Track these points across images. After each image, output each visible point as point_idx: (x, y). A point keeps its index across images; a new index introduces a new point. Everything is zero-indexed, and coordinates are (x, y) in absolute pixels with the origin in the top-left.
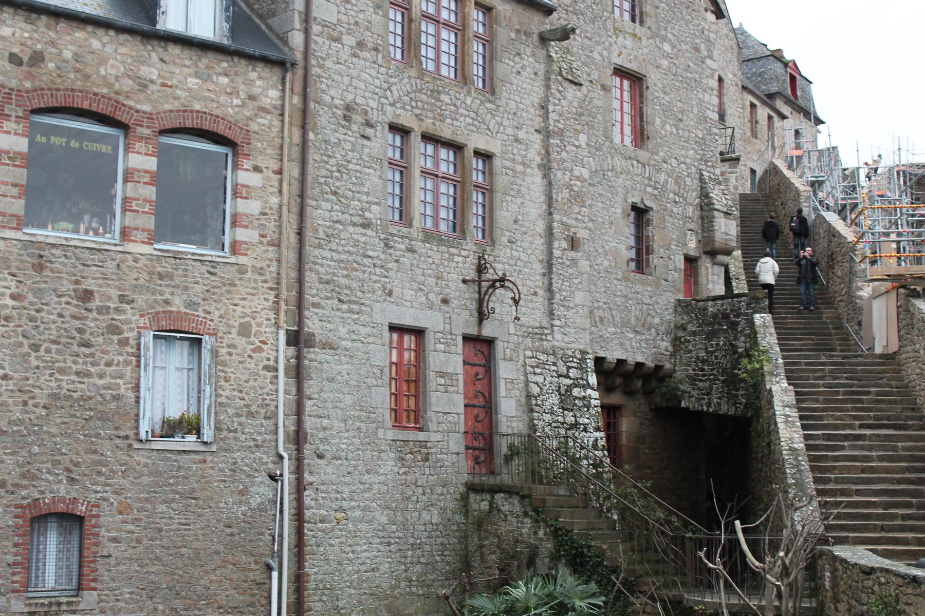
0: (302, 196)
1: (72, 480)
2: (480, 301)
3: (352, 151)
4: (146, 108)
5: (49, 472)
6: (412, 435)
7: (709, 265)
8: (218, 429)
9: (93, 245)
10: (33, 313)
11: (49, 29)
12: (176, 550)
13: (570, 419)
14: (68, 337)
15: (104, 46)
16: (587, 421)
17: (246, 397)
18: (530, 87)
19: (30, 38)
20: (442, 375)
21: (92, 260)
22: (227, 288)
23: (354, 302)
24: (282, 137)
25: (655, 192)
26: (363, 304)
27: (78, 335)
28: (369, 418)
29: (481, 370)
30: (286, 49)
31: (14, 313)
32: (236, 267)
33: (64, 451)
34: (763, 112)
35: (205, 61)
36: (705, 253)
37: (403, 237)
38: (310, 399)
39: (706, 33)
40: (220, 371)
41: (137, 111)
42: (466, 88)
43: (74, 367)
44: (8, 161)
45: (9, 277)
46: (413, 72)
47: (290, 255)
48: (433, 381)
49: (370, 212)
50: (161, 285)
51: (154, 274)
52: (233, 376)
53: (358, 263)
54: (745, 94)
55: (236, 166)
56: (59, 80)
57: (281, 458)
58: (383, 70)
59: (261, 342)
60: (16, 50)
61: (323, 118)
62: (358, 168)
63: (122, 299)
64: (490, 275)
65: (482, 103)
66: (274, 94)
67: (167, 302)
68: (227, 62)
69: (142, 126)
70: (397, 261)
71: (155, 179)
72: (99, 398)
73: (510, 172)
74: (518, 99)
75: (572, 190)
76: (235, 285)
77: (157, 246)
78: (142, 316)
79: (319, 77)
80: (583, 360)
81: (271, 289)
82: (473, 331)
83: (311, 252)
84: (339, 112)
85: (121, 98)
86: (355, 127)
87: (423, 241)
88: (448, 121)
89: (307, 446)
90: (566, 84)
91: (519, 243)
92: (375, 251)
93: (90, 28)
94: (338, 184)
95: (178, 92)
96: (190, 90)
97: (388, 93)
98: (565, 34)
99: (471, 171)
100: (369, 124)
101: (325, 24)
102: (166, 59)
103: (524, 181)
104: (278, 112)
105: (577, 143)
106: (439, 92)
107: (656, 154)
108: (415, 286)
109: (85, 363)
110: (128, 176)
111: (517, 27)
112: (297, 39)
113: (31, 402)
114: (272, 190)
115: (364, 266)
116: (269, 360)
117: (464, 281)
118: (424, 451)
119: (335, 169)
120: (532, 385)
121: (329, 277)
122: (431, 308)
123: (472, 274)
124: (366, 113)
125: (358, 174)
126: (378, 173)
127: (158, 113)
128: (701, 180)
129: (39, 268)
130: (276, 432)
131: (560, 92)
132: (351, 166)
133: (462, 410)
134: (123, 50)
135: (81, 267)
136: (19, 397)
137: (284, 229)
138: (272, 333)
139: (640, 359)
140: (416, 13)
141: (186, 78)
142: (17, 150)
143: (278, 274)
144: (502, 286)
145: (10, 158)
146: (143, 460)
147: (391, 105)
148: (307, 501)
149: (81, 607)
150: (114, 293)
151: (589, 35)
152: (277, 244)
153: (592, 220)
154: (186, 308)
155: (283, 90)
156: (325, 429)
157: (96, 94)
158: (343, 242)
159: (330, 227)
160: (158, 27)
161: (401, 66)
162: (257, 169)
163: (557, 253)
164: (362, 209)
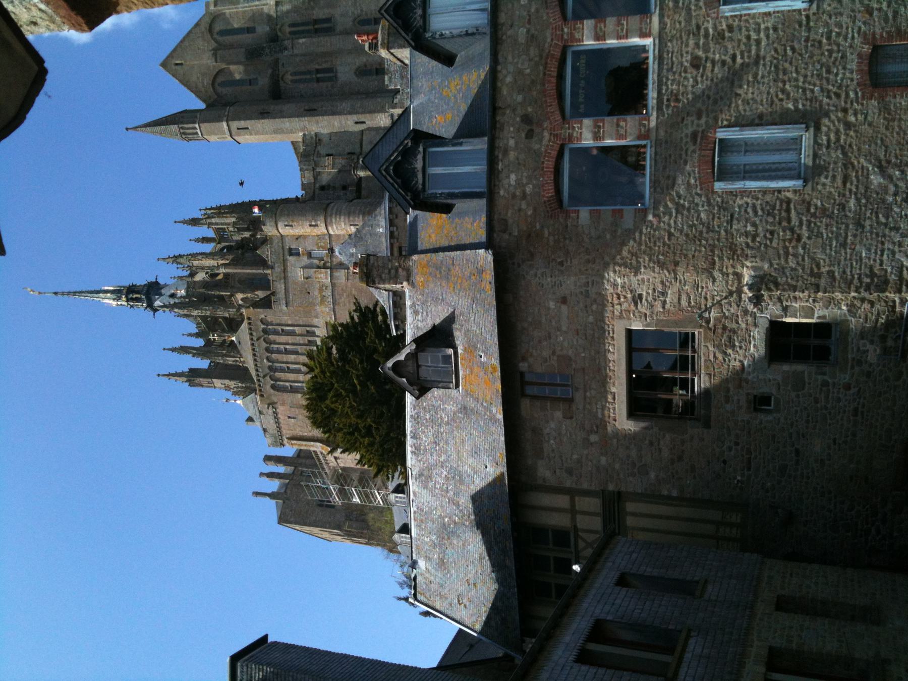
10: (711, 101)
19: (513, 126)
41: (552, 40)
60: (523, 135)
69: (562, 35)
77: (653, 6)
93: (499, 84)
95: (533, 10)
134: (510, 58)
141: (522, 5)
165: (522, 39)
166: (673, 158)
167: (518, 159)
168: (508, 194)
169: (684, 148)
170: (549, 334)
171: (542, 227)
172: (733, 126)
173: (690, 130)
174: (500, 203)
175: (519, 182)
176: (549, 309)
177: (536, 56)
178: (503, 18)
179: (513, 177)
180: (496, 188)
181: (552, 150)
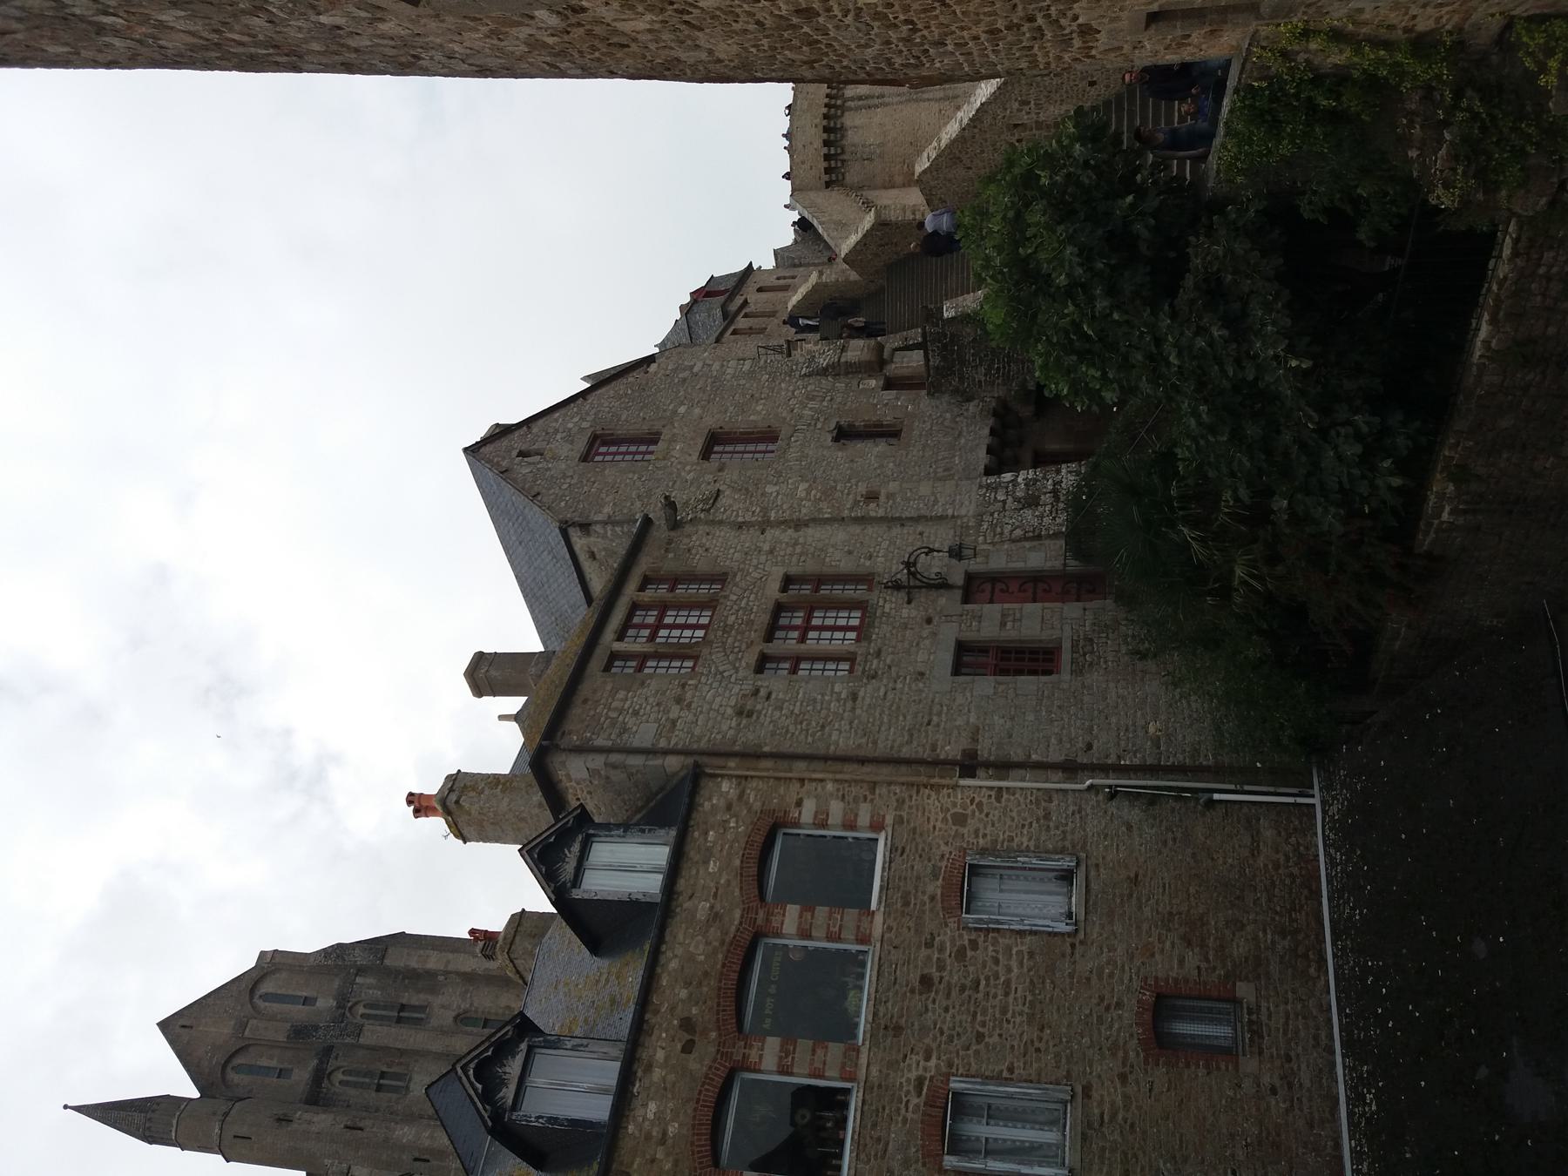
0: (826, 759)
1: (1119, 1005)
2: (930, 587)
3: (782, 709)
4: (737, 914)
5: (1111, 1027)
6: (1066, 656)
7: (893, 366)
8: (1062, 851)
9: (875, 973)
12: (1192, 899)
13: (1047, 498)
14: (969, 1002)
15: (676, 956)
16: (1050, 482)
17: (1029, 821)
18: (720, 539)
19: (666, 1032)
20: (1003, 624)
21: (890, 974)
22: (917, 836)
23: (931, 708)
24: (768, 777)
25: (822, 420)
26: (933, 701)
27: (967, 993)
28: (1049, 697)
29: (999, 586)
30: (682, 774)
31: (944, 1058)
32: (896, 826)
33: (1087, 1012)
34: (741, 323)
35: (692, 854)
36: (881, 370)
37: (866, 662)
38: (1030, 756)
39: (668, 372)
40: (1002, 846)
41: (741, 923)
42: (721, 600)
43: (1000, 997)
44: (790, 1059)
45: (908, 1061)
46: (705, 651)
47: (885, 772)
48: (1011, 633)
49: (841, 693)
50: (915, 904)
51: (903, 912)
52: (1007, 833)
53: (892, 705)
54: (723, 340)
55: (797, 825)
56: (709, 1003)
57: (1091, 787)
58: (703, 679)
59: (972, 804)
60: (679, 1047)
61: (750, 737)
62: (798, 704)
63: (929, 945)
64: (903, 576)
65: (736, 585)
66: (725, 786)
67: (933, 898)
68: (694, 831)
70: (890, 667)
71: (808, 908)
72: (1032, 973)
73: (803, 559)
74: (732, 551)
75: (820, 499)
76: (915, 829)
78: (946, 925)
79: (709, 741)
80: (988, 486)
81: (918, 792)
82: (958, 594)
83: (882, 749)
84: (744, 722)
85: (728, 940)
86: (759, 707)
87: (870, 643)
88: (752, 617)
89: (1079, 760)
90: (718, 505)
91: (872, 550)
92: (879, 689)
93: (659, 970)
94: (814, 724)
95: (722, 881)
97: (726, 674)
98: (670, 504)
99: (802, 595)
100: (756, 692)
101: (659, 735)
102: (690, 892)
103: (811, 545)
104: (743, 782)
105: (774, 494)
106: (726, 626)
107: (785, 419)
108: (913, 649)
109: (996, 986)
110: (805, 934)
111: (663, 552)
112: (673, 763)
113: (1037, 1044)
114: (819, 789)
115: (894, 699)
116: (990, 796)
117: (909, 602)
118: (1082, 643)
119: (799, 727)
120: (1013, 536)
121: (906, 734)
122: (934, 634)
123: (903, 595)
124: (744, 696)
125: (805, 704)
126: (803, 684)
128: (809, 375)
129: (898, 1030)
130: (1065, 791)
131: (725, 510)
132: (796, 711)
133: (1039, 605)
134: (681, 937)
135: (897, 986)
136: (1031, 1057)
137: (858, 778)
138: (962, 792)
139: (987, 431)
140: (648, 648)
141: (710, 873)
142: (778, 1049)
143: (903, 784)
144: (915, 564)
145: (787, 1057)
146: (1097, 929)
147: (737, 673)
148: (1137, 761)
149: (1253, 999)
150: (924, 952)
151: (671, 484)
152: (873, 786)
153: (850, 479)
154: (938, 879)
155: (722, 776)
156: (1060, 741)
157: (724, 965)
158: (871, 720)
159: (856, 732)
160: (659, 900)
161: (700, 662)
162: (799, 803)
163: (881, 513)
164: (838, 701)
165: (701, 915)
166: (887, 1111)
168: (641, 1130)
169: (905, 1099)
172: (973, 1076)
173: (913, 1075)
174: (626, 1145)
175: (659, 1116)
178: (682, 884)
179: (652, 1107)
180: (625, 1119)
181: (716, 1075)
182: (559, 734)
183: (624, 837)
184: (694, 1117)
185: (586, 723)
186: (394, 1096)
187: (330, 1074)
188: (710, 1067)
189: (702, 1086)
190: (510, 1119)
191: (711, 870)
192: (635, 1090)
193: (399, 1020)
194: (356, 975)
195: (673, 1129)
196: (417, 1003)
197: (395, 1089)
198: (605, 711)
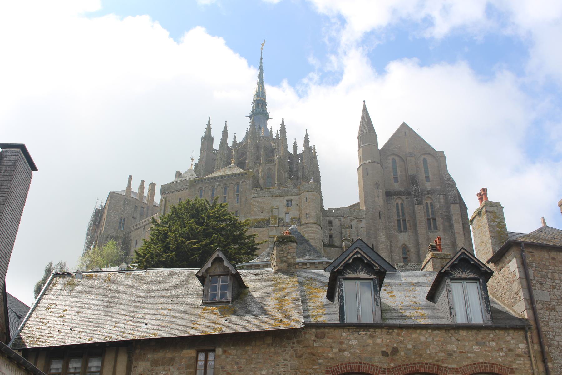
11: (399, 336)
15: (427, 338)
19: (390, 341)
24: (533, 369)
41: (449, 369)
60: (384, 349)
66: (522, 346)
68: (492, 333)
79: (547, 332)
85: (440, 364)
93: (418, 331)
95: (469, 355)
96: (475, 352)
101: (543, 303)
102: (459, 339)
104: (527, 355)
127: (460, 368)
134: (436, 339)
141: (472, 347)
155: (527, 343)
157: (427, 364)
165: (450, 347)
167: (367, 346)
168: (344, 339)
170: (242, 370)
171: (319, 364)
174: (336, 333)
175: (351, 346)
176: (261, 370)
177: (438, 357)
178: (463, 333)
179: (355, 342)
180: (348, 330)
181: (374, 370)
182: (531, 250)
183: (482, 298)
184: (353, 363)
185: (541, 263)
186: (396, 227)
187: (400, 198)
188: (377, 367)
189: (368, 364)
190: (340, 278)
191: (474, 347)
192: (361, 333)
193: (429, 220)
194: (443, 195)
195: (347, 354)
196: (437, 225)
197: (399, 227)
198: (551, 271)
